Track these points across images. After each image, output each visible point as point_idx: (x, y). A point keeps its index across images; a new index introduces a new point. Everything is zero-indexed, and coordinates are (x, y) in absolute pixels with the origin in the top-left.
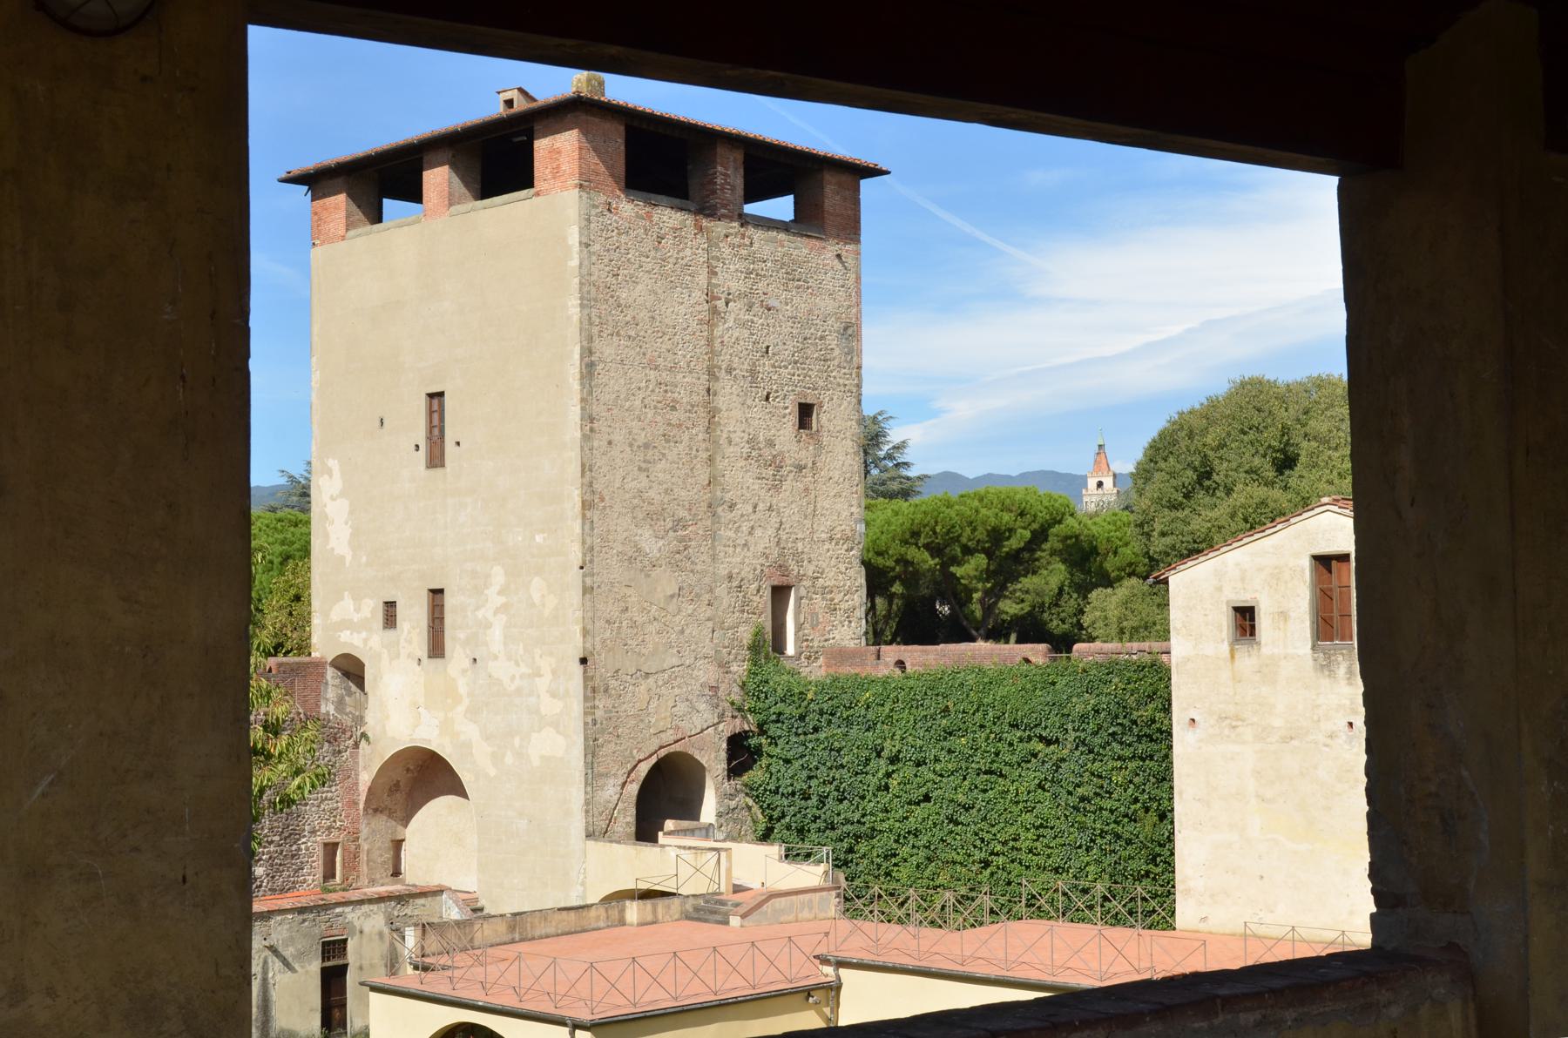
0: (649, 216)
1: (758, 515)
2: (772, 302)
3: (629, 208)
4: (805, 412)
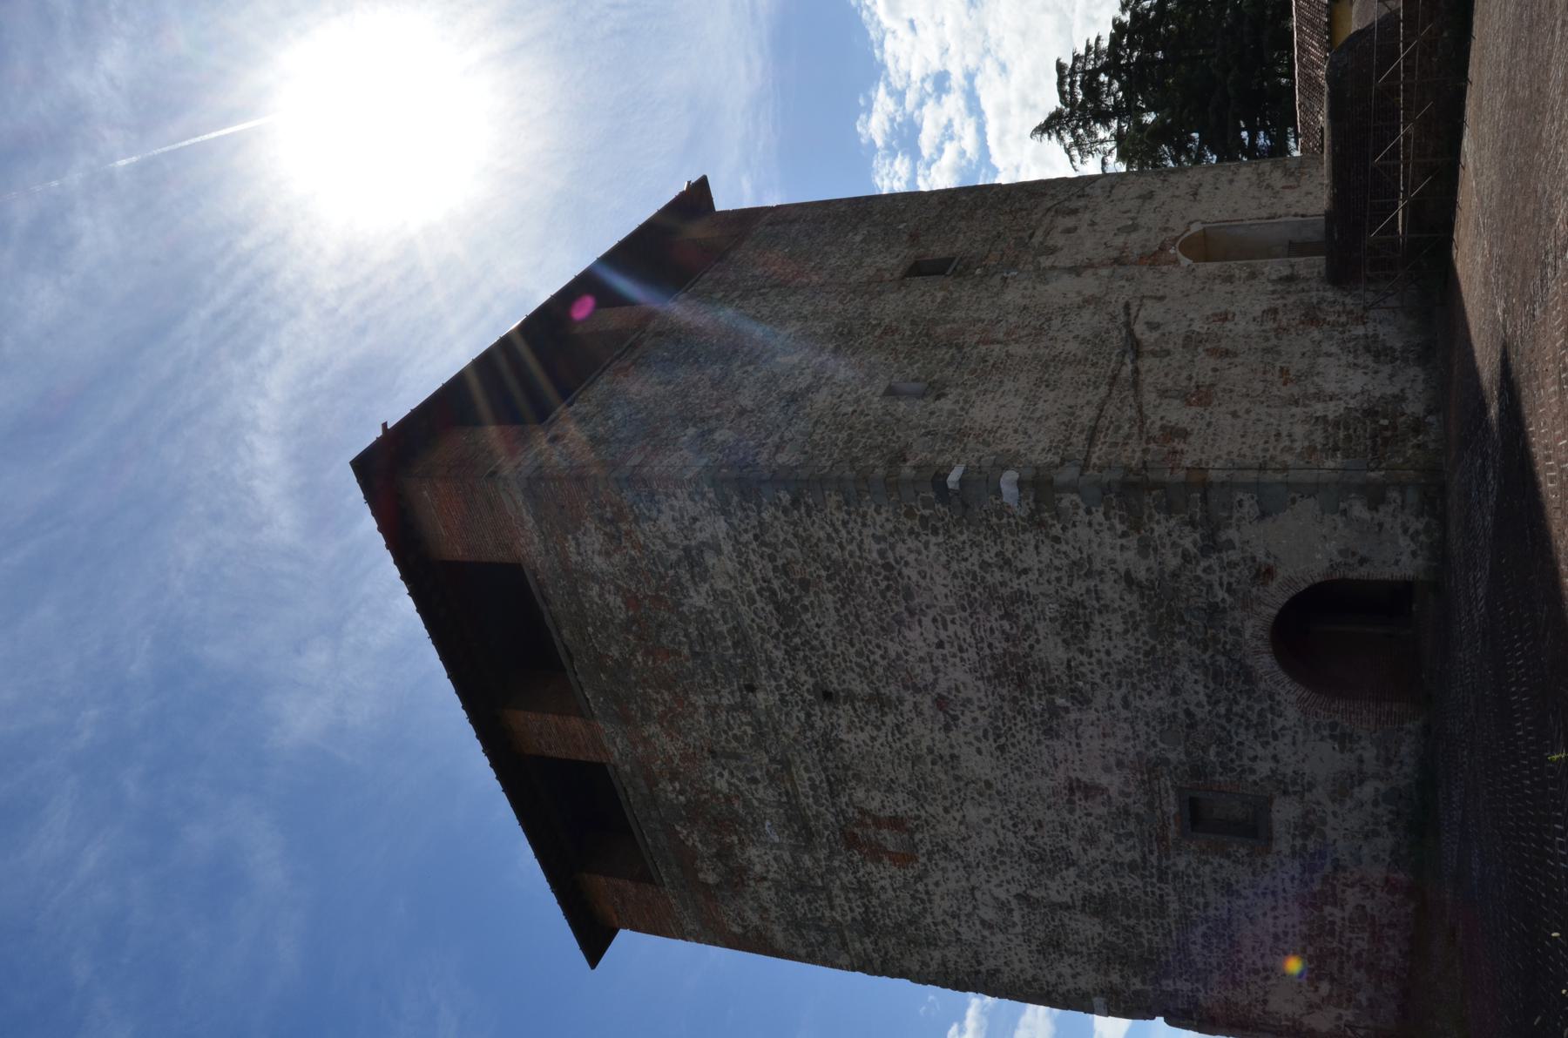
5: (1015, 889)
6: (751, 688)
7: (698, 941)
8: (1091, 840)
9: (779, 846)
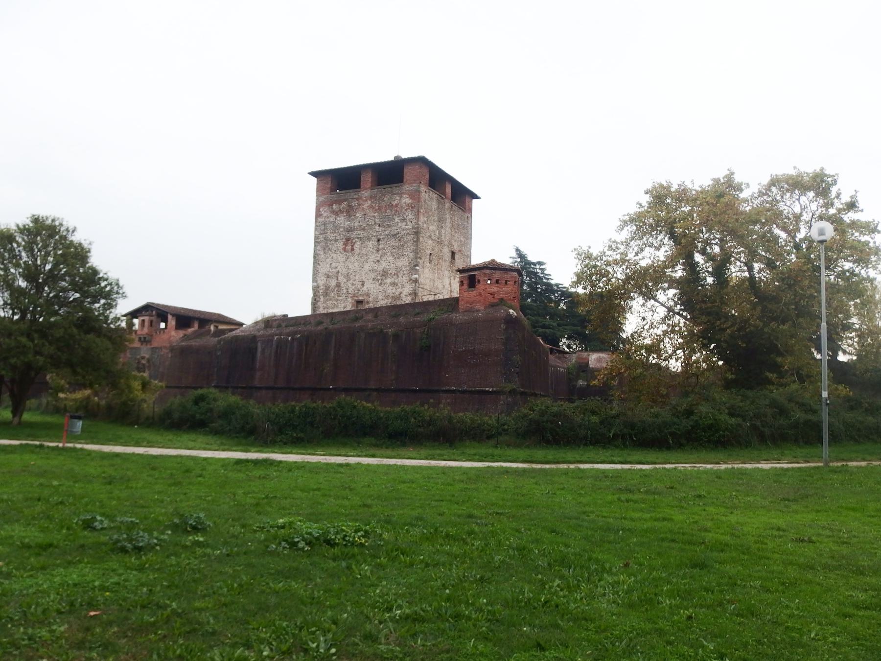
5: (340, 271)
6: (379, 226)
7: (317, 199)
8: (353, 284)
9: (344, 224)
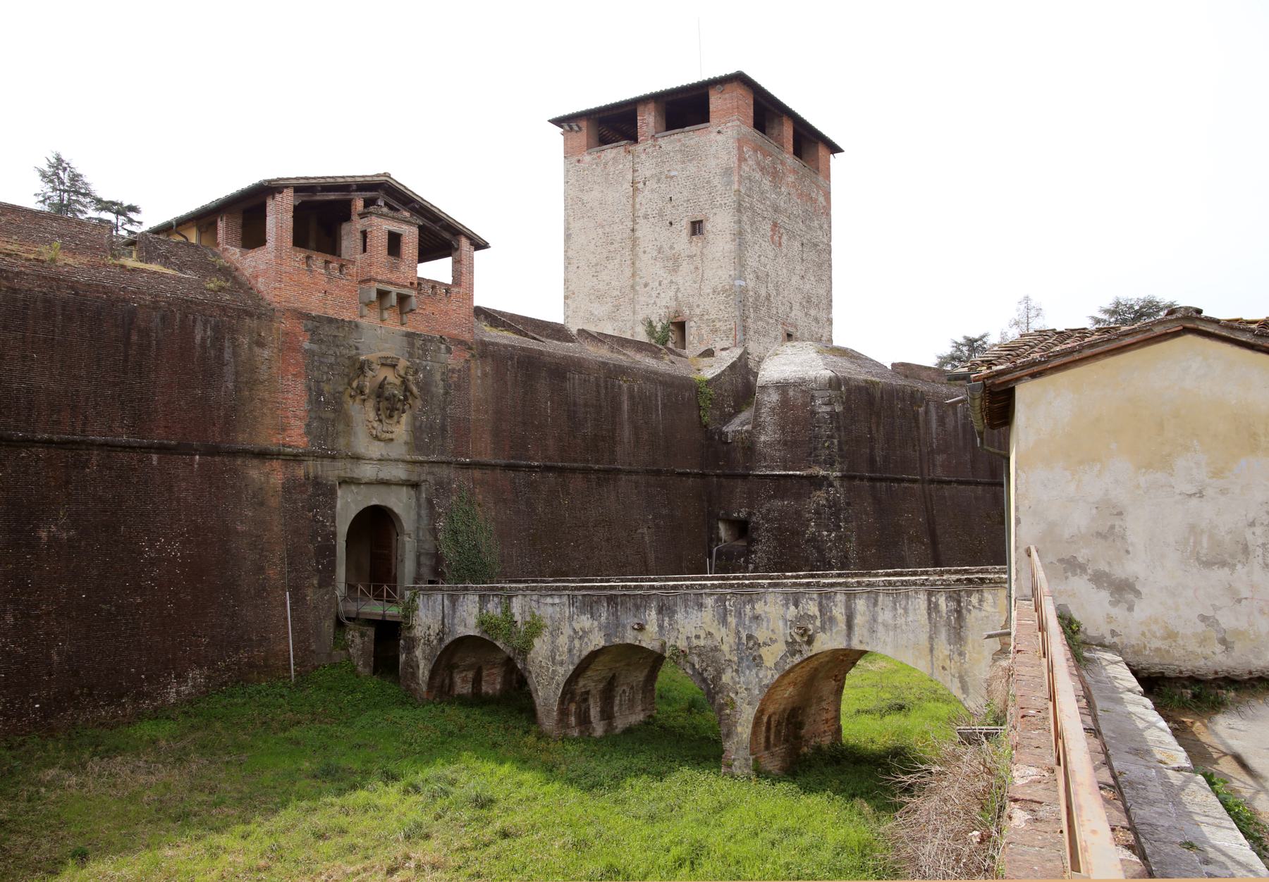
0: (599, 157)
1: (664, 286)
2: (673, 173)
3: (587, 158)
4: (696, 227)
8: (783, 304)
